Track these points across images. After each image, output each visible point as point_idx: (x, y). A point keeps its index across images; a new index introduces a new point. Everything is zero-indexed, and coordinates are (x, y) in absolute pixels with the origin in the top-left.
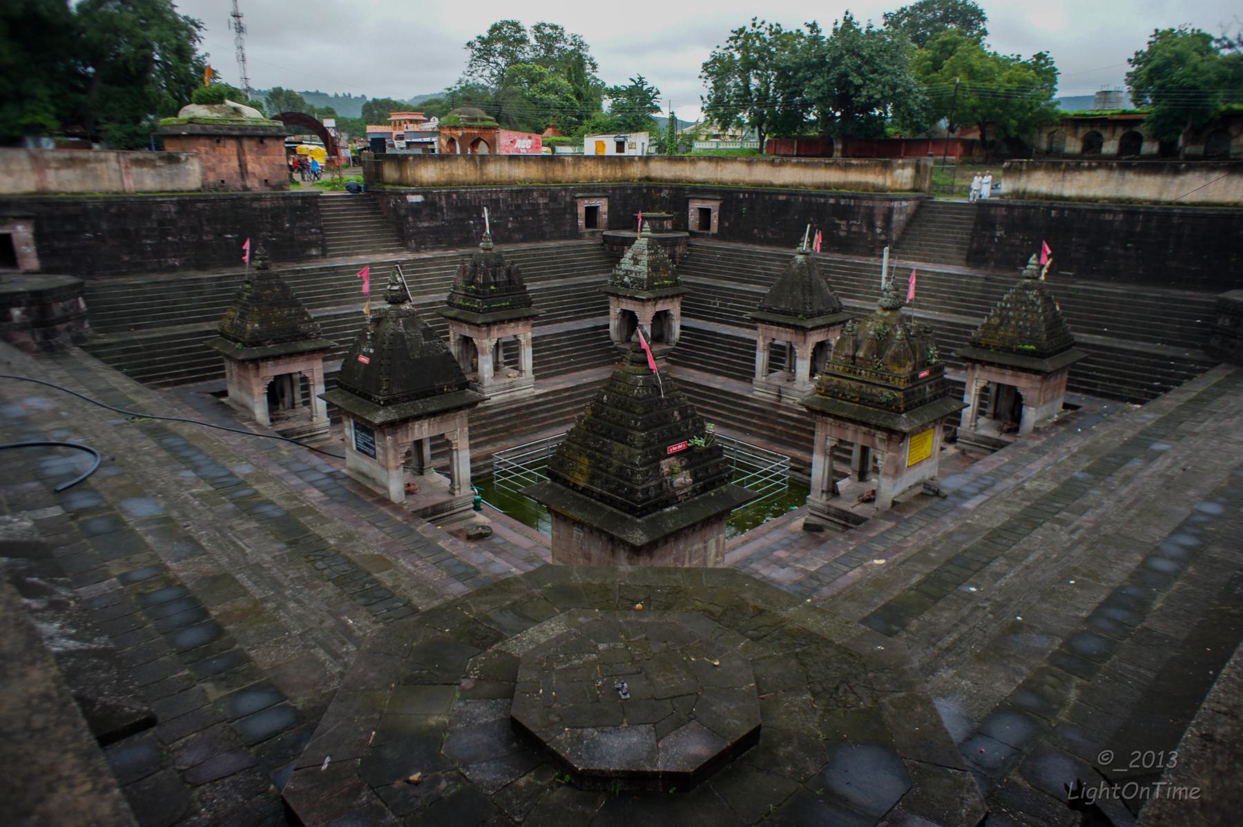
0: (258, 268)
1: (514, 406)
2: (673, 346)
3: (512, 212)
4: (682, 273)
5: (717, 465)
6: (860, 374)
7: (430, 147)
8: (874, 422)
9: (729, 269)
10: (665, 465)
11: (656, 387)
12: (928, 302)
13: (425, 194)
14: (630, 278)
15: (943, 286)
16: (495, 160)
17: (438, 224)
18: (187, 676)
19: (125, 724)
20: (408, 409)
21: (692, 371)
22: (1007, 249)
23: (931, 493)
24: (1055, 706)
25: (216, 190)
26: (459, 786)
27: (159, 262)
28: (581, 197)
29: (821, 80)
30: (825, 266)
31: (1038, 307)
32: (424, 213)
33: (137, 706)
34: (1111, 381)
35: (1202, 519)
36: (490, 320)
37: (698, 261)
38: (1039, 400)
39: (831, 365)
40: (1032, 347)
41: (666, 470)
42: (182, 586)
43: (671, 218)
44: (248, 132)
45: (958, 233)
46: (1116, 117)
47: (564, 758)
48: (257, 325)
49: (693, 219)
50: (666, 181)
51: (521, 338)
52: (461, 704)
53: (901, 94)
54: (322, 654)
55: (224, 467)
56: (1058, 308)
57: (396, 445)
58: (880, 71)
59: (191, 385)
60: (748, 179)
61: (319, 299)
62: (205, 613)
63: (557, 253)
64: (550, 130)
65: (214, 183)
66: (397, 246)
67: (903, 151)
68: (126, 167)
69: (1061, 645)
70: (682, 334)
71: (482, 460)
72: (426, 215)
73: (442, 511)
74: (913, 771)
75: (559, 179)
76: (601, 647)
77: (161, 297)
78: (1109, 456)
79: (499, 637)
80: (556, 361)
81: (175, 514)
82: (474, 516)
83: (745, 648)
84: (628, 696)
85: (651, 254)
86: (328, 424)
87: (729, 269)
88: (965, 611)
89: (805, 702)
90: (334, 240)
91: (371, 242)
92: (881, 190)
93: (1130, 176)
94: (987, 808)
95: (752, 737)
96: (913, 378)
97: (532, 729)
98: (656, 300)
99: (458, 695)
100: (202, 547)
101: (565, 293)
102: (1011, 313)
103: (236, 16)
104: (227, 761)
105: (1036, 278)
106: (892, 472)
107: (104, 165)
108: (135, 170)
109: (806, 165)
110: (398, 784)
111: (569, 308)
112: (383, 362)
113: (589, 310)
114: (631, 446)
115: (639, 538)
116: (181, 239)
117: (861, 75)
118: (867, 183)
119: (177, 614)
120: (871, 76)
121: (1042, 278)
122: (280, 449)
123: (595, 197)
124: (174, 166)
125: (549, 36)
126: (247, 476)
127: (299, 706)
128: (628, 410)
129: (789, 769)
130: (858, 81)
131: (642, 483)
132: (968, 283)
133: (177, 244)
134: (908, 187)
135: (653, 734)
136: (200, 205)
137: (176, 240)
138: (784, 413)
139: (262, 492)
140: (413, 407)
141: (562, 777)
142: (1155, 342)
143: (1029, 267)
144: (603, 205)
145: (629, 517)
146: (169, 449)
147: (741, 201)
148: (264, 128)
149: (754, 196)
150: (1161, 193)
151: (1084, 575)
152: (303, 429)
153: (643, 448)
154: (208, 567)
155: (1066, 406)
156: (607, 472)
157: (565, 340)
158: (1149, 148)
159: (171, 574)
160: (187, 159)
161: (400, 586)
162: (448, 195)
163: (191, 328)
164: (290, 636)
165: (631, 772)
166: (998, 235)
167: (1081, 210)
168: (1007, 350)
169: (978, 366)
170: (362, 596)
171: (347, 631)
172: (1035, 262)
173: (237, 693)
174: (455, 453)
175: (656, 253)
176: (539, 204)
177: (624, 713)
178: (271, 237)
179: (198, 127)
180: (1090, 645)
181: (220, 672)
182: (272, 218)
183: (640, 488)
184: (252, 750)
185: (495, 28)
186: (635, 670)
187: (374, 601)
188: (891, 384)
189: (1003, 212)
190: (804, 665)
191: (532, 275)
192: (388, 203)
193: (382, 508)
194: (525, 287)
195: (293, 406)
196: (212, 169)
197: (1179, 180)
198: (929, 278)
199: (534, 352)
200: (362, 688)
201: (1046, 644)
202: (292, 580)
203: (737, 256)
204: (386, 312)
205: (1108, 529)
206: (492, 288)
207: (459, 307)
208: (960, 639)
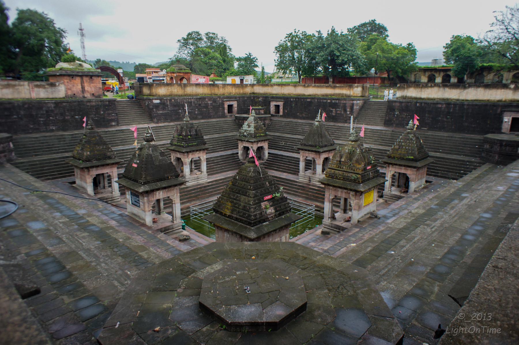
0: (89, 129)
1: (199, 187)
2: (265, 161)
3: (197, 107)
4: (268, 131)
5: (285, 205)
6: (343, 168)
7: (163, 81)
8: (349, 188)
9: (288, 129)
10: (263, 205)
11: (259, 172)
12: (369, 141)
13: (161, 100)
14: (247, 133)
15: (375, 135)
16: (190, 86)
17: (166, 112)
18: (55, 293)
19: (26, 292)
20: (154, 186)
21: (273, 171)
22: (400, 119)
23: (373, 217)
24: (429, 294)
25: (72, 98)
26: (177, 332)
27: (46, 128)
28: (226, 101)
29: (323, 53)
30: (327, 127)
31: (414, 141)
32: (160, 107)
33: (31, 285)
34: (444, 171)
35: (483, 219)
36: (188, 150)
37: (275, 126)
38: (416, 179)
39: (331, 165)
40: (412, 157)
41: (263, 207)
42: (54, 256)
43: (263, 109)
44: (85, 74)
45: (380, 113)
46: (440, 68)
47: (222, 318)
48: (88, 153)
49: (272, 109)
50: (261, 94)
51: (201, 158)
52: (177, 299)
53: (355, 59)
54: (116, 283)
55: (73, 211)
56: (422, 142)
57: (149, 201)
58: (347, 50)
59: (60, 179)
60: (294, 93)
61: (115, 143)
62: (64, 267)
63: (216, 124)
64: (212, 75)
65: (71, 95)
66: (149, 121)
67: (357, 82)
68: (32, 88)
69: (430, 270)
70: (269, 156)
71: (185, 209)
72: (161, 108)
73: (169, 230)
74: (372, 319)
75: (217, 93)
76: (238, 273)
77: (47, 143)
78: (445, 199)
79: (194, 271)
80: (216, 168)
81: (51, 228)
82: (182, 232)
83: (299, 273)
84: (250, 292)
85: (255, 123)
86: (119, 195)
87: (288, 129)
88: (390, 261)
89: (325, 293)
90: (123, 119)
91: (138, 120)
92: (349, 96)
93: (447, 89)
94: (404, 333)
95: (303, 307)
96: (365, 169)
97: (209, 307)
98: (258, 142)
99: (176, 295)
100: (64, 241)
101: (220, 140)
102: (403, 144)
103: (81, 30)
104: (73, 328)
105: (412, 129)
106: (357, 208)
107: (22, 87)
108: (36, 89)
109: (318, 87)
110: (150, 332)
111: (221, 146)
112: (143, 166)
113: (230, 147)
114: (249, 197)
115: (253, 235)
116: (56, 119)
117: (339, 51)
118: (343, 94)
119: (51, 268)
120: (343, 52)
121: (415, 129)
122: (98, 205)
123: (232, 101)
124: (53, 88)
125: (211, 38)
126: (84, 214)
127: (106, 304)
128: (247, 182)
129: (320, 320)
130: (338, 54)
131: (254, 212)
132: (385, 133)
133: (54, 120)
134: (360, 95)
135: (261, 307)
136: (64, 104)
137: (54, 119)
138: (312, 187)
139: (90, 220)
140: (156, 185)
141: (222, 327)
142: (460, 155)
143: (409, 125)
144: (235, 104)
145: (248, 227)
146: (49, 204)
147: (292, 102)
148: (92, 72)
149: (297, 99)
150: (459, 96)
151: (438, 242)
152: (108, 197)
153: (254, 197)
154: (65, 249)
155: (427, 182)
156: (238, 208)
157: (220, 159)
158: (454, 80)
159: (49, 252)
160: (59, 85)
161: (150, 258)
162: (170, 100)
163: (60, 155)
164: (102, 276)
165: (252, 323)
167: (429, 103)
168: (402, 159)
169: (391, 166)
170: (134, 262)
171: (128, 276)
172: (412, 123)
173: (77, 299)
174: (174, 205)
175: (257, 123)
176: (208, 104)
177: (248, 299)
178: (95, 117)
179: (64, 71)
180: (442, 269)
181: (71, 291)
182: (96, 109)
183: (253, 214)
184: (84, 323)
185: (189, 34)
186: (252, 282)
187: (139, 264)
188: (356, 172)
189: (398, 104)
190: (324, 279)
191: (206, 133)
192: (145, 103)
193: (143, 228)
194: (203, 137)
195: (104, 188)
196: (70, 89)
197: (466, 91)
198: (369, 131)
199: (207, 164)
200: (134, 293)
201: (424, 270)
202: (103, 256)
203: (291, 124)
204: (144, 145)
205: (447, 225)
206: (189, 137)
207: (175, 145)
208: (388, 271)
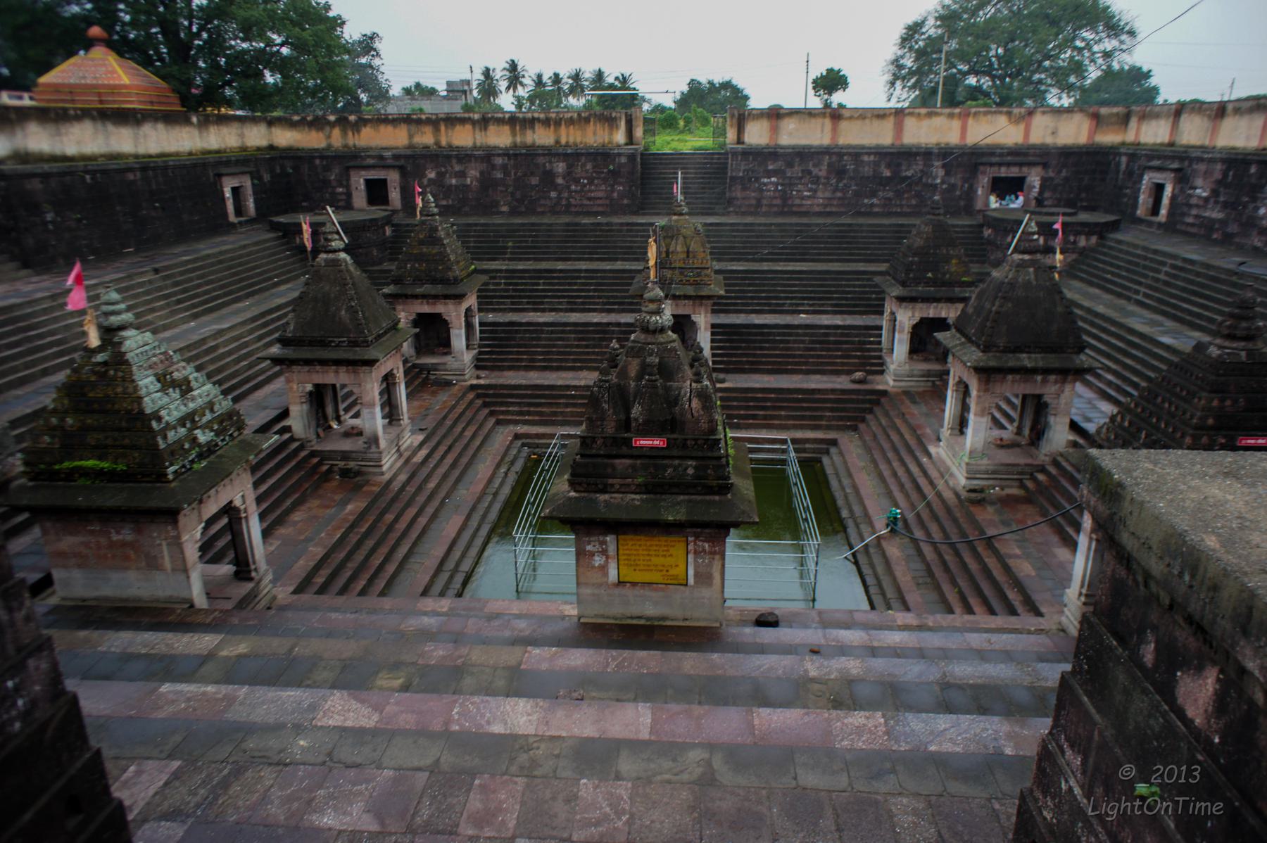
14: (208, 426)
132: (150, 282)
166: (49, 217)
